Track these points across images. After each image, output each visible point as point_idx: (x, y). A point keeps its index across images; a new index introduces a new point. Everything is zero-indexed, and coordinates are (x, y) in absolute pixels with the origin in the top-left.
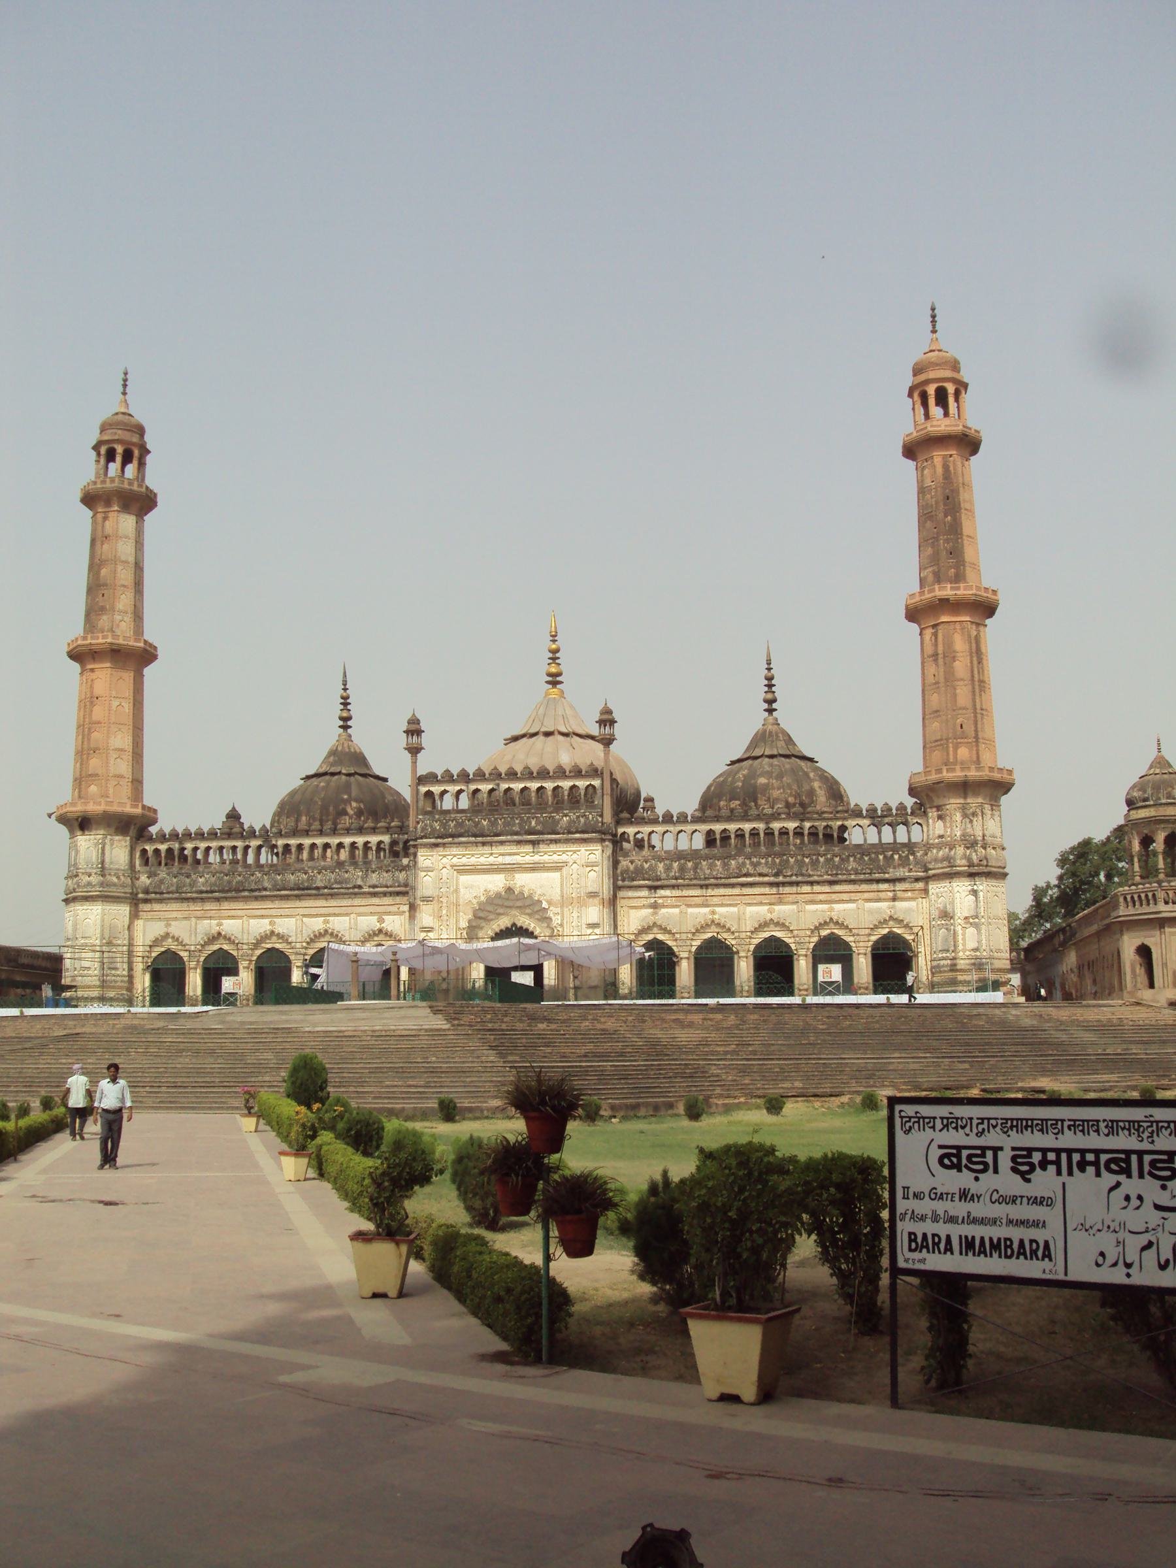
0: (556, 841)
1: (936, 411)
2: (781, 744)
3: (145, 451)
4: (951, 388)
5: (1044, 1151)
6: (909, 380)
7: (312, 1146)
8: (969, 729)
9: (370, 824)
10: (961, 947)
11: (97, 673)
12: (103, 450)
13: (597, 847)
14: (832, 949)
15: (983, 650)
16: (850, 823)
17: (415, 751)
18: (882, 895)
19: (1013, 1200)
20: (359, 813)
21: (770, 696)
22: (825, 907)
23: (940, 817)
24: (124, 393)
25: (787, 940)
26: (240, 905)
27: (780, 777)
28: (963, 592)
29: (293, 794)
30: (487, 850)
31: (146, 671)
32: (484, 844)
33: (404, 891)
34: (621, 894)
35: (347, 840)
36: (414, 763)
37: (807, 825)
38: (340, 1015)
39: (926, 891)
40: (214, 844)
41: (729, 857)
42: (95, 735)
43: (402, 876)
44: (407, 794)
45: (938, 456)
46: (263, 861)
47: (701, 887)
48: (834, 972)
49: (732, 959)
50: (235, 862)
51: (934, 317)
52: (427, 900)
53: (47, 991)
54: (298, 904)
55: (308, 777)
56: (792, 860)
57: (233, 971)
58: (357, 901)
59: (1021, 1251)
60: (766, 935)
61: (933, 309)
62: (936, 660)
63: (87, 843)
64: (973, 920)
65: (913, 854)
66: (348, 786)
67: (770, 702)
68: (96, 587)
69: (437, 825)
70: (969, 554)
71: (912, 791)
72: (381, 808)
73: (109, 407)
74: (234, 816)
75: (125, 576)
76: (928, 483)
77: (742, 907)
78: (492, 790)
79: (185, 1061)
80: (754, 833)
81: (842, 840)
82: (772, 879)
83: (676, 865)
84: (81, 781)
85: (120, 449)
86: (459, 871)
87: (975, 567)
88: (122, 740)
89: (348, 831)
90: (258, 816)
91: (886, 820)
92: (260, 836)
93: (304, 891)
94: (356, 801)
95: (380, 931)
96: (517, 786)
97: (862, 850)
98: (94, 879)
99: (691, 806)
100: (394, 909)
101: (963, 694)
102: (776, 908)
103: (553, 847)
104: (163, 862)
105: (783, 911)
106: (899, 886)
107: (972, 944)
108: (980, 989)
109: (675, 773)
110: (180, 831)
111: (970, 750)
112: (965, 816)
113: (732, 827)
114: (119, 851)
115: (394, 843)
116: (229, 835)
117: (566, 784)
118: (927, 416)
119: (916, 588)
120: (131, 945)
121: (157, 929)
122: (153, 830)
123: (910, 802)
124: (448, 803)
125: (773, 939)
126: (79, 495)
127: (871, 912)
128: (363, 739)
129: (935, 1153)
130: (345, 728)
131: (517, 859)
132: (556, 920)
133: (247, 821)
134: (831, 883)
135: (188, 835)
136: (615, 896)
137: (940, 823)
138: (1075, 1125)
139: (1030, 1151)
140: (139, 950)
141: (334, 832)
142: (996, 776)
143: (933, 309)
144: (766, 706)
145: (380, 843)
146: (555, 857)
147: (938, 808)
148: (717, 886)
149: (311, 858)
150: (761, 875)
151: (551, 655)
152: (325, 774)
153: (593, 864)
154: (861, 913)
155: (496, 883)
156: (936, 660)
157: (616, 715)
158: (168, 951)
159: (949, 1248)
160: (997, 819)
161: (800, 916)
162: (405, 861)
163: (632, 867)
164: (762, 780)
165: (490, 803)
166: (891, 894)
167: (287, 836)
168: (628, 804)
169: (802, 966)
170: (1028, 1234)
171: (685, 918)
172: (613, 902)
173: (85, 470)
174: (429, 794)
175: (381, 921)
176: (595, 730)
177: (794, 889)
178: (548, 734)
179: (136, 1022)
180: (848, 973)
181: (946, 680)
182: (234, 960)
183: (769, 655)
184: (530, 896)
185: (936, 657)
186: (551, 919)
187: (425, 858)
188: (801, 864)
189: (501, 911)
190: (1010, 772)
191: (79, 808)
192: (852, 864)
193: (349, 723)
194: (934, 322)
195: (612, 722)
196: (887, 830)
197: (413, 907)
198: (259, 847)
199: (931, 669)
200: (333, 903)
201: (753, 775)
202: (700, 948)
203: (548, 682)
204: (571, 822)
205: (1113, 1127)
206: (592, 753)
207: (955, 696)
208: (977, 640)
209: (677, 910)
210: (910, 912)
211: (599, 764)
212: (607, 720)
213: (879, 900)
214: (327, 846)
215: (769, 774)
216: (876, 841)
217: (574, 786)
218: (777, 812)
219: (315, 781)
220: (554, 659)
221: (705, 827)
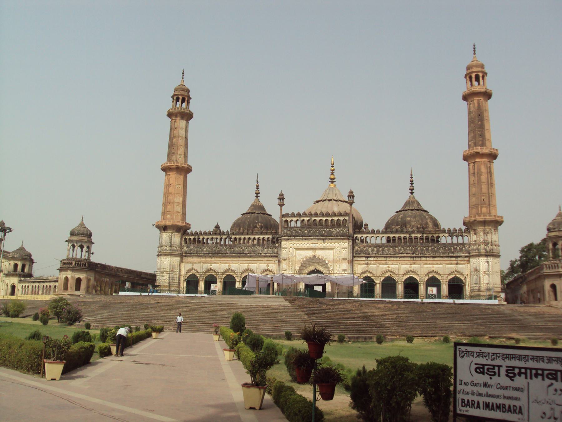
0: (332, 239)
1: (475, 83)
2: (416, 205)
3: (189, 98)
4: (481, 75)
5: (520, 368)
6: (465, 72)
7: (236, 348)
8: (487, 201)
9: (265, 231)
10: (482, 283)
11: (171, 176)
12: (175, 98)
13: (346, 242)
14: (433, 282)
15: (492, 171)
16: (441, 235)
17: (281, 205)
18: (452, 262)
19: (506, 388)
20: (261, 227)
21: (412, 188)
22: (431, 266)
23: (475, 234)
24: (183, 78)
25: (416, 278)
26: (218, 259)
27: (415, 217)
28: (485, 150)
29: (238, 220)
30: (306, 241)
31: (188, 175)
32: (305, 239)
33: (276, 256)
34: (355, 259)
35: (257, 237)
36: (281, 210)
37: (425, 235)
38: (252, 299)
39: (469, 261)
40: (210, 237)
41: (395, 246)
42: (170, 197)
43: (276, 250)
44: (278, 221)
45: (476, 100)
46: (227, 243)
47: (385, 257)
48: (434, 290)
49: (396, 284)
50: (217, 243)
51: (474, 48)
52: (284, 259)
53: (150, 286)
54: (239, 259)
55: (244, 214)
56: (419, 248)
57: (215, 282)
58: (260, 259)
59: (509, 410)
60: (409, 276)
62: (474, 175)
63: (166, 235)
64: (487, 273)
65: (465, 247)
66: (258, 217)
67: (412, 190)
68: (171, 145)
69: (289, 232)
70: (487, 136)
71: (465, 224)
72: (269, 226)
73: (177, 83)
74: (217, 227)
75: (182, 142)
76: (472, 110)
77: (400, 265)
78: (309, 220)
79: (195, 314)
80: (405, 238)
81: (438, 241)
82: (411, 255)
83: (375, 249)
84: (164, 213)
85: (181, 97)
86: (298, 249)
87: (490, 141)
88: (179, 199)
89: (257, 234)
90: (226, 227)
91: (455, 234)
92: (226, 235)
93: (241, 255)
94: (261, 223)
95: (268, 270)
96: (318, 219)
97: (446, 245)
98: (168, 248)
99: (382, 227)
100: (272, 262)
101: (484, 188)
102: (413, 266)
103: (330, 241)
104: (193, 243)
105: (415, 267)
106: (459, 259)
107: (486, 282)
108: (489, 299)
109: (376, 215)
110: (198, 232)
111: (487, 208)
112: (484, 233)
113: (397, 236)
114: (177, 239)
115: (273, 238)
116: (215, 234)
117: (336, 218)
118: (472, 85)
119: (467, 148)
120: (180, 272)
121: (189, 266)
122: (189, 231)
123: (463, 228)
124: (293, 224)
125: (411, 278)
126: (166, 113)
127: (448, 268)
128: (264, 201)
129: (474, 367)
130: (257, 197)
131: (317, 245)
132: (331, 268)
133: (222, 229)
134: (433, 257)
135: (201, 233)
136: (353, 260)
137: (475, 236)
138: (533, 358)
139: (514, 368)
140: (183, 273)
141: (252, 234)
142: (497, 219)
144: (410, 191)
145: (268, 238)
146: (331, 245)
147: (474, 230)
148: (391, 257)
149: (244, 243)
150: (407, 253)
152: (250, 213)
153: (345, 248)
154: (444, 269)
155: (310, 254)
156: (474, 175)
157: (354, 194)
158: (193, 274)
159: (478, 406)
160: (497, 235)
161: (421, 269)
162: (277, 245)
163: (359, 249)
164: (408, 219)
165: (308, 225)
166: (456, 262)
167: (235, 235)
168: (358, 226)
169: (422, 288)
170: (513, 403)
171: (378, 269)
172: (352, 262)
173: (169, 104)
174: (286, 221)
175: (268, 266)
176: (347, 199)
177: (419, 259)
178: (330, 200)
179: (180, 299)
180: (439, 291)
181: (478, 182)
182: (216, 278)
183: (411, 172)
184: (322, 259)
185: (474, 174)
187: (284, 244)
188: (422, 250)
189: (311, 264)
190: (502, 217)
191: (163, 223)
192: (441, 250)
194: (474, 50)
195: (353, 196)
196: (455, 238)
197: (279, 262)
198: (226, 238)
199: (472, 179)
200: (251, 259)
201: (405, 217)
202: (384, 280)
204: (337, 232)
205: (550, 360)
206: (345, 207)
207: (481, 188)
208: (490, 168)
209: (375, 266)
210: (463, 269)
211: (348, 211)
212: (351, 195)
213: (451, 264)
214: (249, 239)
215: (411, 217)
216: (451, 242)
217: (339, 219)
218: (413, 230)
219: (246, 215)
221: (387, 235)
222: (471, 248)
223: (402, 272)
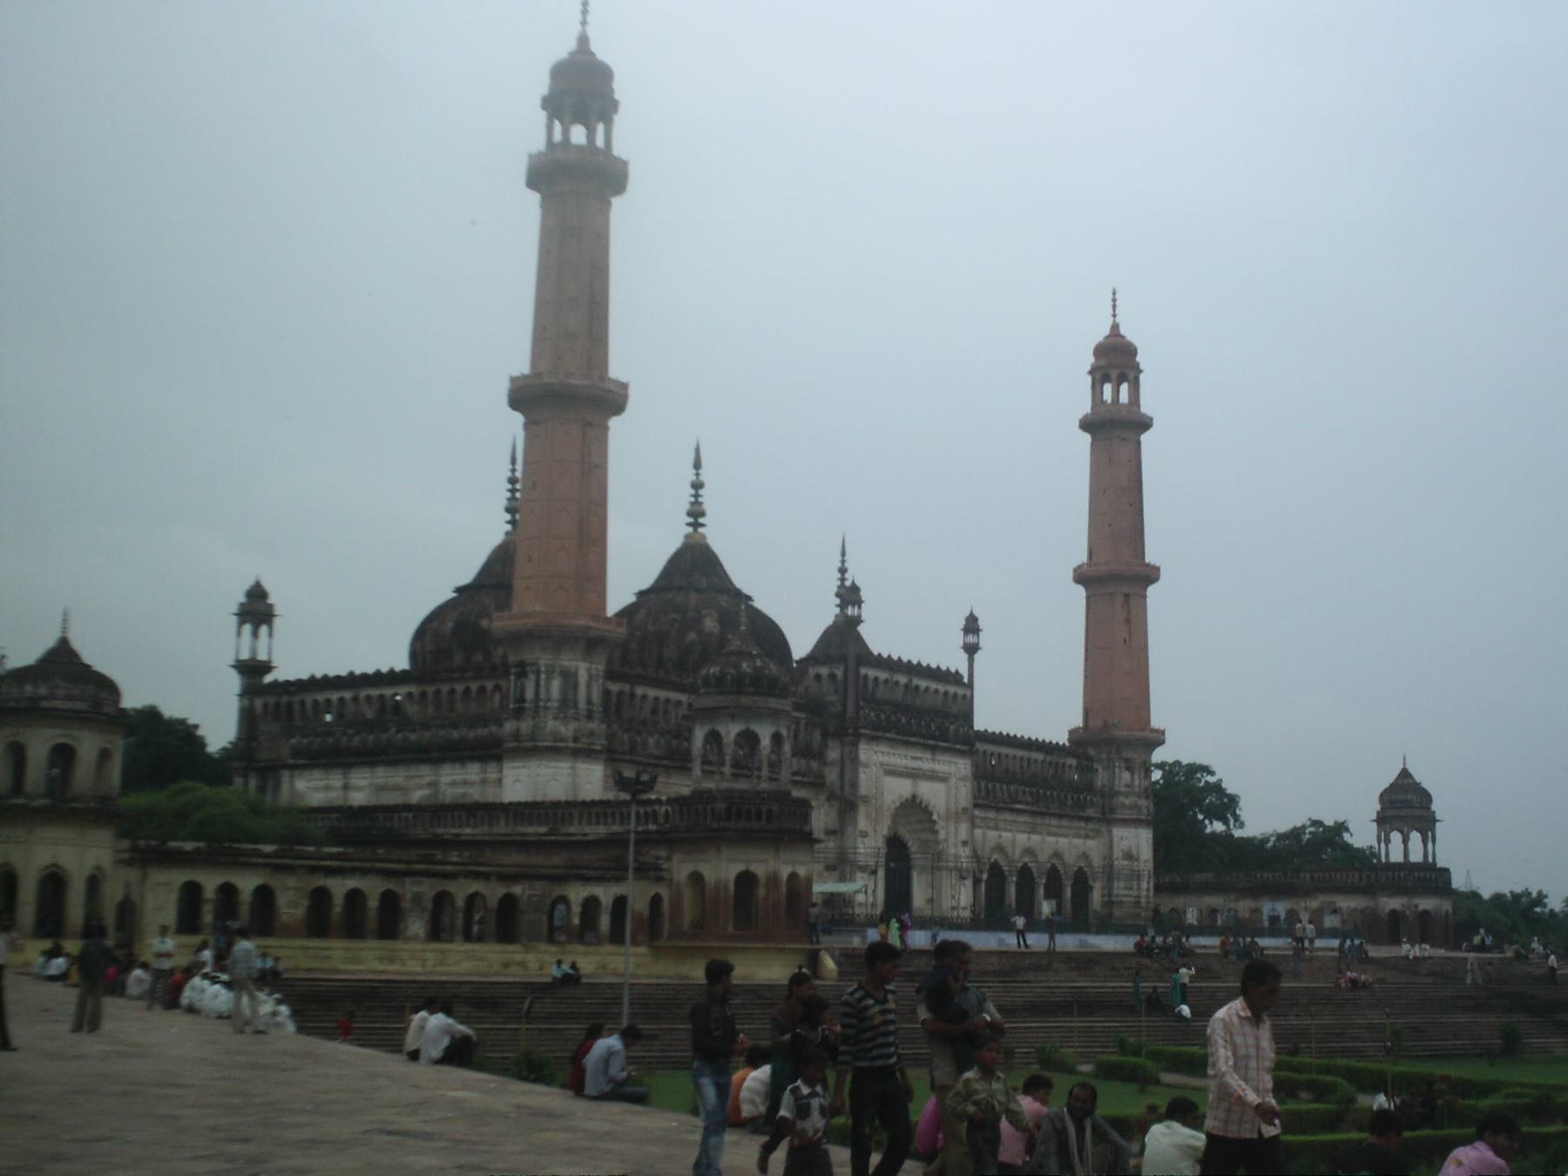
23: (1128, 769)
30: (902, 751)
32: (906, 744)
43: (814, 764)
47: (998, 809)
52: (865, 800)
78: (906, 686)
102: (1034, 837)
106: (1091, 826)
117: (952, 689)
132: (942, 835)
134: (1060, 816)
153: (964, 779)
157: (981, 624)
186: (936, 832)
203: (689, 524)
217: (955, 695)
220: (696, 496)
223: (1018, 853)
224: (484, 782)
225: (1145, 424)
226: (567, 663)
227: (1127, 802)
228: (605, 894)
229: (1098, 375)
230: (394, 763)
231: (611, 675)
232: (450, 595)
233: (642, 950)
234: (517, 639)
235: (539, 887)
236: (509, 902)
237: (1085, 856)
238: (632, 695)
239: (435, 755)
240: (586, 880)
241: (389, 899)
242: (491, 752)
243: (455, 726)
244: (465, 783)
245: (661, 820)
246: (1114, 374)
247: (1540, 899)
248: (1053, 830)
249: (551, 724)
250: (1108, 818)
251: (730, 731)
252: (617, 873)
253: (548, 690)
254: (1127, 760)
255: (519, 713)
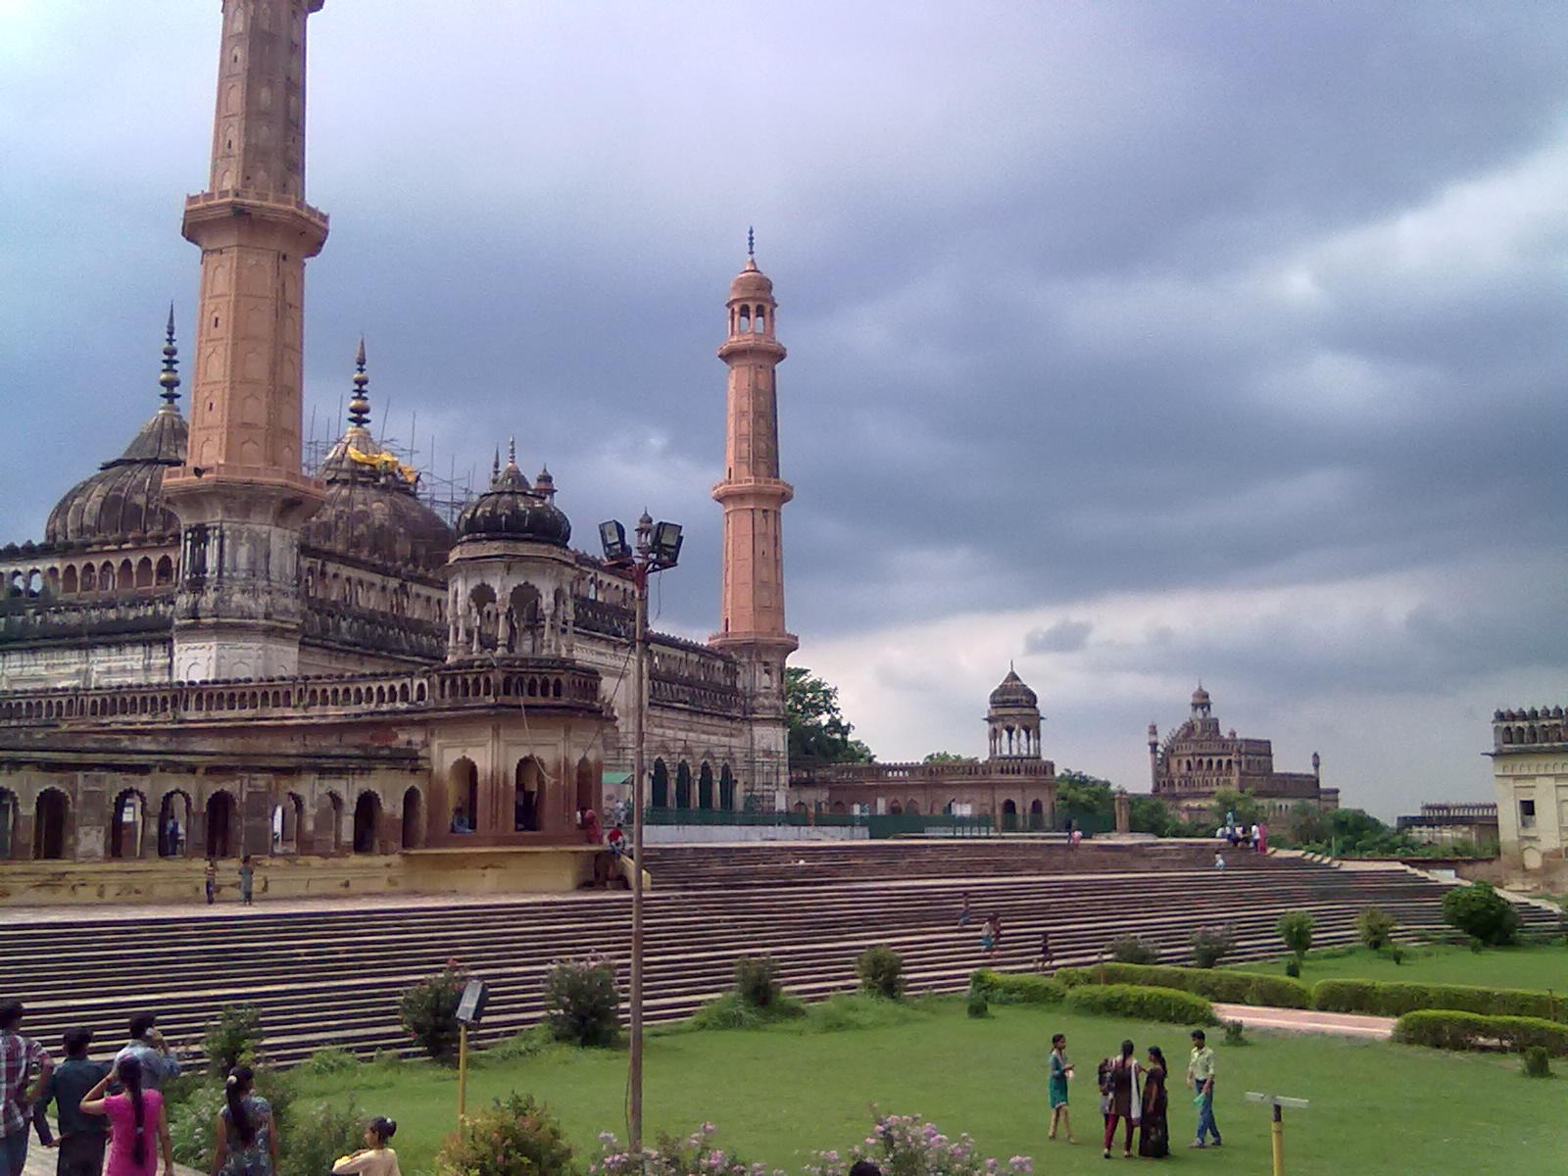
23: (766, 671)
32: (592, 638)
47: (663, 707)
61: (751, 232)
102: (692, 735)
106: (735, 725)
132: (622, 730)
134: (712, 715)
143: (751, 232)
147: (766, 664)
150: (686, 703)
151: (357, 387)
193: (176, 390)
203: (351, 420)
220: (360, 391)
222: (755, 703)
224: (147, 669)
225: (780, 355)
226: (257, 528)
227: (766, 702)
228: (349, 790)
229: (737, 309)
230: (34, 650)
231: (305, 550)
232: (95, 471)
233: (395, 859)
234: (192, 498)
235: (262, 781)
236: (220, 805)
237: (730, 756)
238: (323, 574)
239: (86, 639)
240: (323, 772)
241: (52, 806)
242: (156, 634)
243: (111, 604)
244: (124, 670)
245: (413, 695)
246: (752, 307)
247: (1107, 784)
248: (705, 728)
249: (237, 598)
250: (749, 717)
251: (501, 586)
252: (365, 764)
253: (234, 560)
254: (766, 664)
255: (197, 585)
